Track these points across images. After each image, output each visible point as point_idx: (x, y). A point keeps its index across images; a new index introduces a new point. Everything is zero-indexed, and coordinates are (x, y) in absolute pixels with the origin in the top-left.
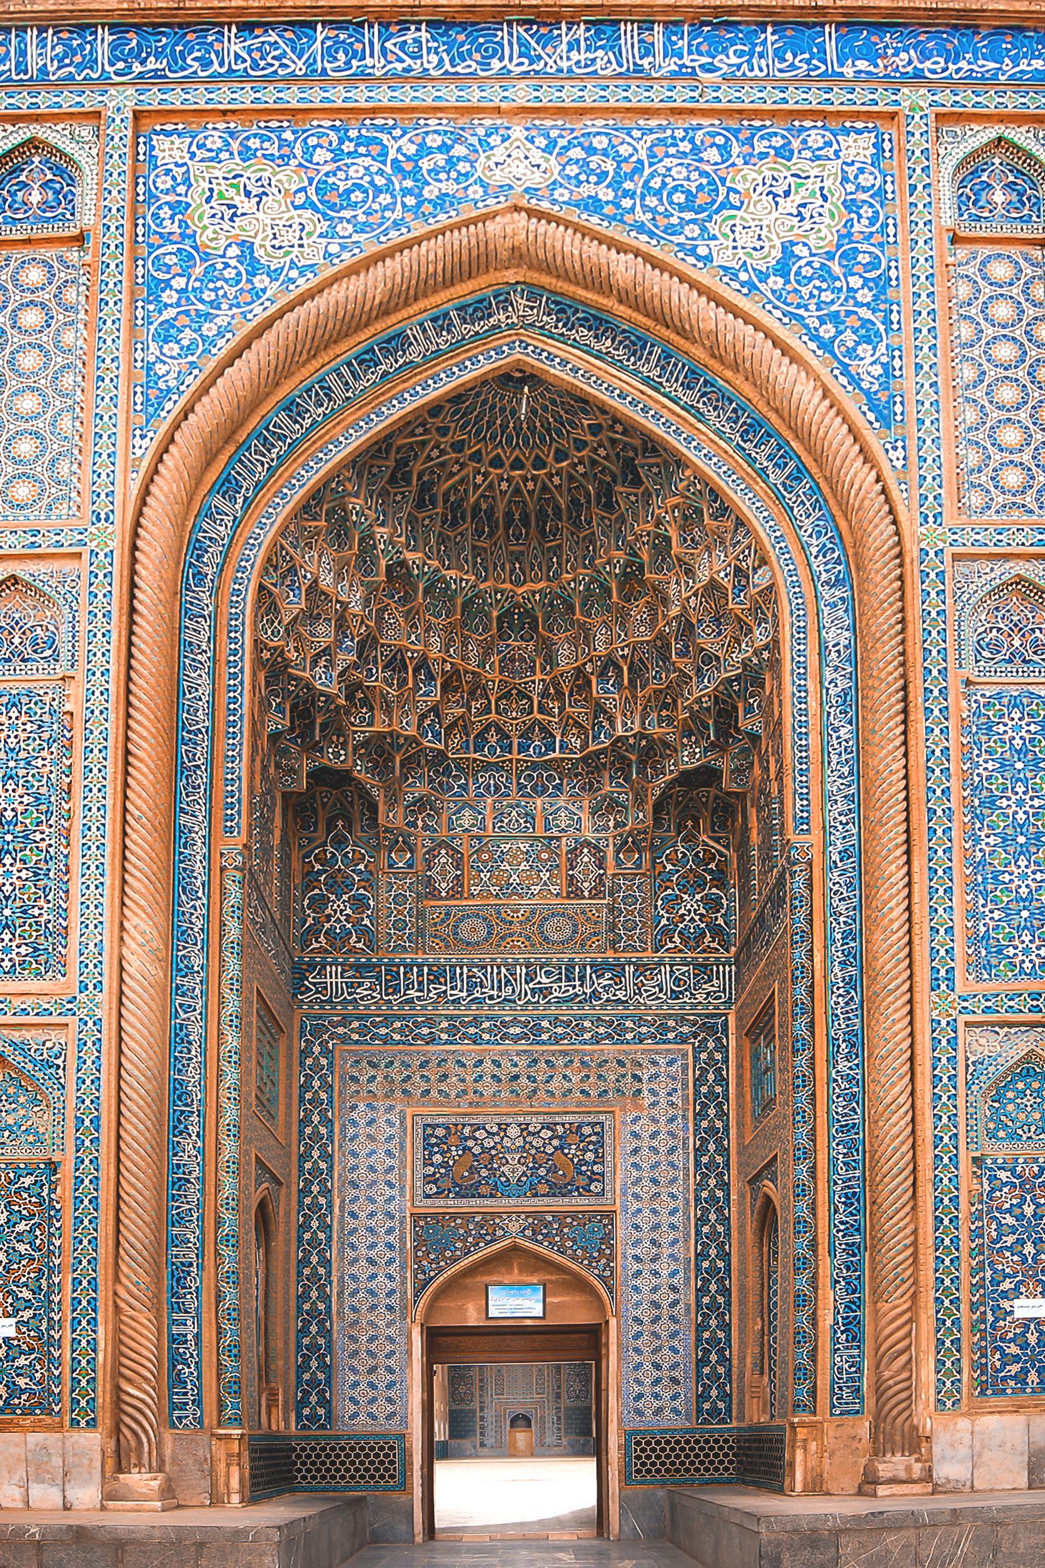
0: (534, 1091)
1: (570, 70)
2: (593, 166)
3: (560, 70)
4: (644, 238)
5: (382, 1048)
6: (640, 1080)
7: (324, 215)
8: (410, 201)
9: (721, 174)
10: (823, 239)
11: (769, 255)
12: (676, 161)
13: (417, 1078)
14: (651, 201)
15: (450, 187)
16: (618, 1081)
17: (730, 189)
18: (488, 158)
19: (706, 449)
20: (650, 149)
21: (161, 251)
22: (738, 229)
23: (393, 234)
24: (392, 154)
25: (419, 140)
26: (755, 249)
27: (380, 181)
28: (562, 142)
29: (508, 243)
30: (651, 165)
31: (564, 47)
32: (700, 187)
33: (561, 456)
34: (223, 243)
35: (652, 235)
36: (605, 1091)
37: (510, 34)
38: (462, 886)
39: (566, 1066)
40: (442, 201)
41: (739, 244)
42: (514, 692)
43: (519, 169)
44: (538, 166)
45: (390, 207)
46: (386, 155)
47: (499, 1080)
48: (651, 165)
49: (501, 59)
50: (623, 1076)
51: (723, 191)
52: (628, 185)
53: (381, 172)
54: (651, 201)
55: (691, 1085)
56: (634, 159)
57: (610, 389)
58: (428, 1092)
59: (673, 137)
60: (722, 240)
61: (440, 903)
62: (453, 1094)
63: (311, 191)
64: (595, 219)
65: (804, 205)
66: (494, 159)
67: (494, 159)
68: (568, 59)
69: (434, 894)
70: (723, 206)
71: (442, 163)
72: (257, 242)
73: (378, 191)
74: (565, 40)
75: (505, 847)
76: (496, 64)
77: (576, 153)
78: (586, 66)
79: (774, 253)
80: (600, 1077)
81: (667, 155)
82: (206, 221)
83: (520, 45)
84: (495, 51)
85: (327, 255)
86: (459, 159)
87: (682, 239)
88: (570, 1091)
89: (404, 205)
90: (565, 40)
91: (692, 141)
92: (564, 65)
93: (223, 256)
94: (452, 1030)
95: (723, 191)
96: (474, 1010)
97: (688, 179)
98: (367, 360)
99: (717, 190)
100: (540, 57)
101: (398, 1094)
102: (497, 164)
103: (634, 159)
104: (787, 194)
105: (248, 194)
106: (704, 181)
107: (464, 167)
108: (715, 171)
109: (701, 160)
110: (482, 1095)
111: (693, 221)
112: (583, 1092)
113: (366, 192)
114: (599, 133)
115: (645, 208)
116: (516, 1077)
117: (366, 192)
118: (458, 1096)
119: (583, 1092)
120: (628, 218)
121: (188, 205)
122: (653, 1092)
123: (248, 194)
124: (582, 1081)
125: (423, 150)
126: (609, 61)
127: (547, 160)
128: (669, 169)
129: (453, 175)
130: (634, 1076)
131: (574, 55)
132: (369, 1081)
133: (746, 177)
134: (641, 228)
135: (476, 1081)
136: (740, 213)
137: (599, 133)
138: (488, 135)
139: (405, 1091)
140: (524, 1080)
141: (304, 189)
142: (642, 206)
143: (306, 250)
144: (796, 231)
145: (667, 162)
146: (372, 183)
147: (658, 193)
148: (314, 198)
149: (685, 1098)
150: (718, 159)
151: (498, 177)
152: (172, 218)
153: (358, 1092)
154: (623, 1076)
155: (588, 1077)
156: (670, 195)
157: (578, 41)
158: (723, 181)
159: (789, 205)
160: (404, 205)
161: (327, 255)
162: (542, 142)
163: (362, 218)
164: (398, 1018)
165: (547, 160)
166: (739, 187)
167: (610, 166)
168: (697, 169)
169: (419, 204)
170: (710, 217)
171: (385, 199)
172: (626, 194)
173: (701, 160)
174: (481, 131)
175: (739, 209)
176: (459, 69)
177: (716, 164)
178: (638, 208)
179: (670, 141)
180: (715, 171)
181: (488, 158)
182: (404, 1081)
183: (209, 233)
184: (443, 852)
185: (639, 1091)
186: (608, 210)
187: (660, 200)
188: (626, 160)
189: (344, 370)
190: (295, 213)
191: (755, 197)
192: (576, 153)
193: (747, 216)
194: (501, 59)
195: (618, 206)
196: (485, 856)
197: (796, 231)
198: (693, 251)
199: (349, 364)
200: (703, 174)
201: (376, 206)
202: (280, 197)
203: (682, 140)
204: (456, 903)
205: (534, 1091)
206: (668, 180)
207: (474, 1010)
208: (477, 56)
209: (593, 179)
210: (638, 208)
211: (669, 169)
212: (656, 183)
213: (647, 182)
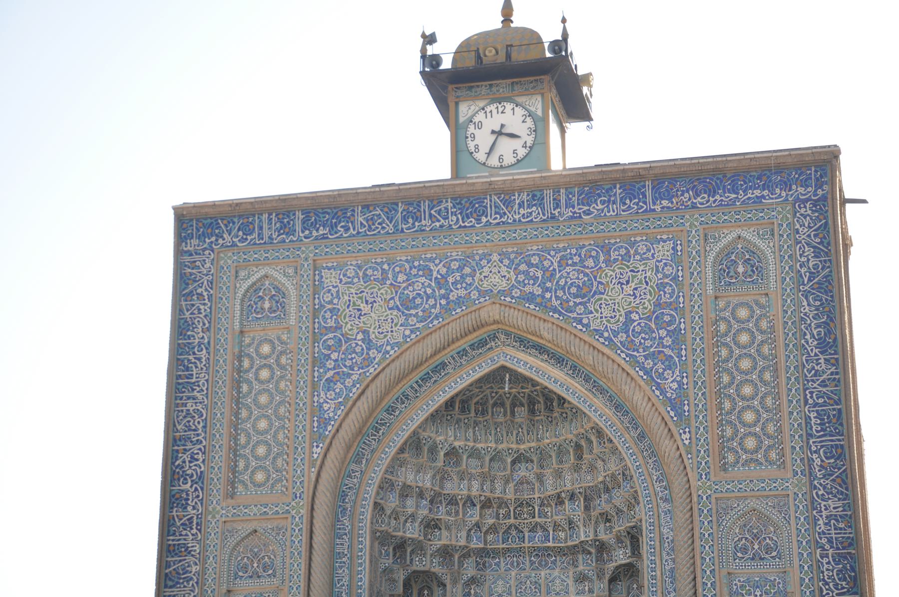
1: (520, 221)
2: (532, 274)
3: (515, 221)
4: (556, 316)
7: (403, 313)
8: (443, 302)
9: (595, 273)
10: (646, 308)
11: (619, 320)
12: (572, 268)
14: (560, 293)
15: (462, 293)
17: (600, 283)
18: (481, 274)
19: (597, 411)
20: (559, 262)
21: (326, 337)
22: (604, 305)
23: (436, 322)
24: (435, 274)
25: (447, 265)
26: (611, 317)
27: (429, 291)
28: (517, 261)
29: (491, 319)
30: (560, 271)
31: (517, 206)
32: (584, 283)
34: (355, 331)
35: (560, 314)
37: (491, 201)
40: (459, 301)
41: (604, 315)
43: (495, 279)
44: (505, 276)
45: (434, 306)
46: (432, 275)
48: (560, 271)
49: (486, 217)
51: (595, 284)
52: (548, 285)
53: (430, 286)
54: (560, 293)
56: (551, 269)
57: (549, 378)
59: (571, 254)
60: (595, 314)
63: (397, 299)
64: (532, 307)
65: (636, 289)
66: (484, 274)
67: (484, 274)
68: (519, 213)
70: (595, 293)
71: (458, 278)
72: (371, 330)
73: (428, 297)
74: (517, 202)
76: (484, 219)
77: (523, 267)
78: (528, 217)
79: (621, 319)
81: (568, 265)
82: (347, 320)
83: (496, 207)
84: (484, 212)
85: (405, 336)
86: (467, 275)
87: (575, 315)
89: (440, 304)
90: (517, 202)
91: (580, 256)
92: (517, 217)
93: (355, 339)
95: (595, 284)
97: (578, 278)
98: (425, 378)
99: (592, 284)
100: (505, 214)
102: (485, 277)
103: (551, 269)
104: (628, 282)
105: (367, 302)
106: (586, 279)
107: (469, 280)
108: (592, 272)
109: (584, 267)
111: (580, 303)
113: (422, 298)
114: (534, 254)
115: (557, 298)
117: (422, 298)
120: (549, 305)
121: (339, 310)
123: (367, 302)
125: (450, 272)
126: (539, 213)
127: (509, 273)
128: (568, 274)
129: (464, 285)
131: (522, 211)
133: (609, 274)
134: (555, 310)
136: (604, 297)
137: (534, 254)
138: (481, 260)
141: (392, 298)
142: (556, 297)
143: (394, 334)
144: (633, 305)
145: (568, 269)
146: (425, 292)
147: (563, 288)
148: (398, 303)
150: (593, 264)
151: (486, 285)
152: (331, 318)
156: (569, 288)
157: (523, 202)
158: (595, 277)
159: (628, 289)
160: (440, 304)
161: (405, 336)
162: (506, 262)
163: (421, 314)
165: (509, 273)
166: (604, 281)
167: (539, 274)
168: (582, 272)
169: (448, 303)
170: (589, 300)
171: (431, 302)
172: (548, 290)
173: (584, 267)
174: (477, 258)
175: (603, 294)
176: (466, 224)
177: (592, 268)
178: (553, 298)
179: (569, 256)
180: (592, 272)
181: (481, 274)
183: (349, 326)
186: (538, 300)
187: (564, 292)
188: (547, 270)
189: (415, 385)
190: (389, 312)
191: (611, 286)
192: (523, 267)
193: (608, 298)
194: (486, 217)
195: (543, 297)
197: (633, 305)
198: (580, 322)
199: (417, 382)
200: (586, 275)
201: (427, 306)
202: (382, 303)
203: (575, 255)
206: (568, 280)
208: (475, 215)
209: (531, 282)
210: (553, 298)
211: (568, 274)
212: (562, 282)
213: (558, 282)
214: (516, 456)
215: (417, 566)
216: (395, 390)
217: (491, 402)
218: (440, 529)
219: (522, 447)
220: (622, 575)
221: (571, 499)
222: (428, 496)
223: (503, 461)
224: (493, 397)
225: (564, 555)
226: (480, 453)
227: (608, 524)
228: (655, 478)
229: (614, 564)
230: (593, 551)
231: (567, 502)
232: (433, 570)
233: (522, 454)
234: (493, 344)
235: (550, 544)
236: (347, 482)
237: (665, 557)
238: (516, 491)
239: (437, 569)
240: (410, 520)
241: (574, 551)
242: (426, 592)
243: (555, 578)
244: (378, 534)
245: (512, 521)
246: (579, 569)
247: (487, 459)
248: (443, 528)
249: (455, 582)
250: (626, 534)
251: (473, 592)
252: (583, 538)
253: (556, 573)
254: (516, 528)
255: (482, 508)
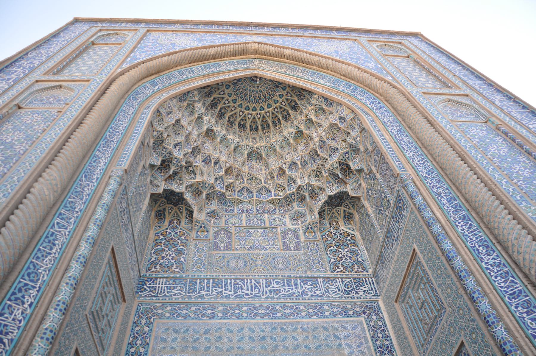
0: (276, 347)
5: (183, 321)
6: (339, 339)
13: (203, 339)
16: (326, 339)
33: (269, 106)
36: (320, 346)
38: (231, 245)
39: (293, 331)
42: (254, 178)
47: (254, 340)
50: (329, 336)
55: (370, 340)
58: (209, 348)
61: (220, 252)
62: (225, 349)
69: (217, 248)
75: (252, 231)
80: (314, 337)
88: (298, 346)
94: (225, 313)
96: (238, 301)
101: (190, 349)
110: (243, 350)
112: (306, 346)
116: (264, 338)
118: (228, 350)
119: (306, 346)
122: (349, 346)
124: (304, 340)
130: (335, 336)
132: (172, 341)
135: (239, 341)
139: (194, 348)
140: (269, 340)
149: (369, 348)
153: (164, 348)
154: (329, 336)
155: (307, 337)
164: (194, 304)
182: (194, 341)
184: (223, 232)
185: (340, 345)
196: (242, 235)
199: (201, 67)
204: (228, 252)
205: (276, 347)
207: (238, 301)
214: (251, 150)
215: (175, 187)
216: (186, 66)
217: (238, 119)
218: (195, 174)
219: (255, 146)
220: (326, 213)
221: (289, 167)
222: (192, 144)
223: (242, 154)
224: (240, 116)
225: (282, 206)
226: (229, 142)
227: (317, 178)
228: (369, 103)
229: (323, 201)
230: (307, 194)
231: (286, 170)
232: (185, 197)
233: (254, 151)
234: (251, 65)
235: (273, 197)
236: (141, 89)
237: (389, 129)
238: (249, 170)
239: (188, 196)
240: (178, 148)
241: (288, 200)
242: (175, 222)
243: (275, 218)
244: (155, 133)
245: (245, 184)
246: (294, 210)
247: (232, 147)
248: (198, 173)
249: (200, 211)
250: (338, 165)
251: (212, 222)
252: (300, 183)
253: (276, 216)
254: (248, 189)
255: (226, 172)
